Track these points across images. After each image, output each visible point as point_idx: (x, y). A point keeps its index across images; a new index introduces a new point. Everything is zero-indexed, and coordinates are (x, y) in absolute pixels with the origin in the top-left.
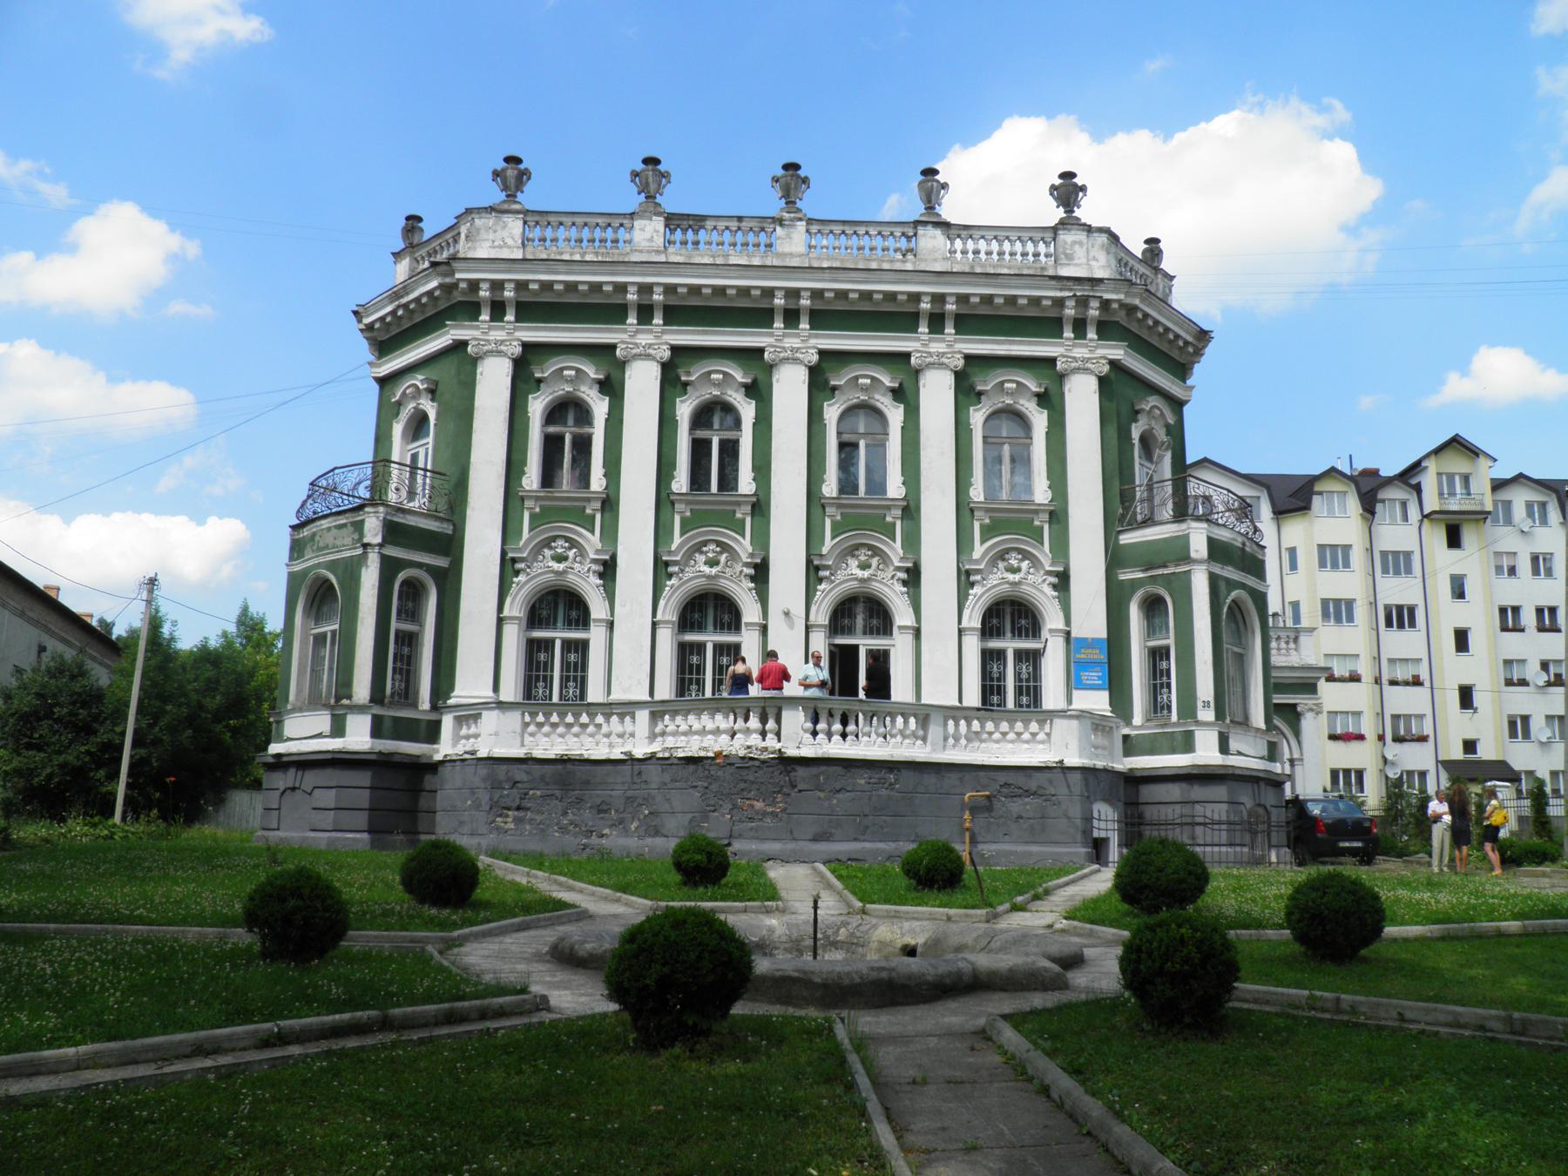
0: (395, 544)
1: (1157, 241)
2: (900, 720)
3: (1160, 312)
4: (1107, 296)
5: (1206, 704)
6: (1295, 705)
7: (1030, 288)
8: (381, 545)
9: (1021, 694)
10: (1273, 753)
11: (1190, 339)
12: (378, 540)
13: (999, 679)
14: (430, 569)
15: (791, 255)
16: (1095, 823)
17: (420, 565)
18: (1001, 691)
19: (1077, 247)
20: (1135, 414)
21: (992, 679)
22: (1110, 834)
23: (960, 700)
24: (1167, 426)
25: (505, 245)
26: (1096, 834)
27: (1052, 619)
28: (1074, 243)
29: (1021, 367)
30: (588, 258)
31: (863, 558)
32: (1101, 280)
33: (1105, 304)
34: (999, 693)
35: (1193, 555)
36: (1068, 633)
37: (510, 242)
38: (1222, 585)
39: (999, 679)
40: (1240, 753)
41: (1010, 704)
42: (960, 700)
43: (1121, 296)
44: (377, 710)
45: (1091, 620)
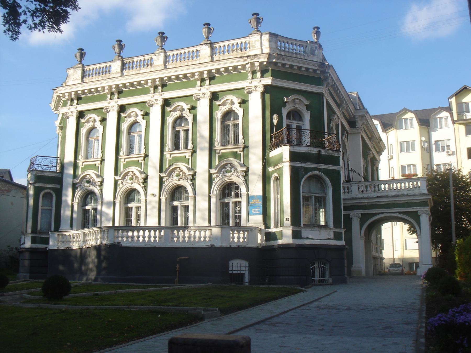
0: (40, 182)
1: (318, 28)
2: (152, 232)
3: (291, 61)
4: (261, 60)
5: (287, 220)
6: (417, 211)
7: (232, 62)
8: (34, 183)
9: (236, 218)
10: (337, 236)
11: (316, 68)
12: (33, 182)
13: (238, 213)
14: (53, 189)
15: (158, 66)
16: (231, 269)
17: (49, 188)
18: (228, 217)
19: (256, 42)
20: (284, 104)
21: (226, 214)
22: (244, 272)
23: (210, 222)
24: (307, 105)
25: (77, 79)
26: (231, 272)
27: (243, 189)
28: (256, 41)
29: (233, 94)
30: (100, 79)
31: (177, 173)
32: (257, 55)
33: (261, 63)
34: (239, 219)
35: (284, 160)
36: (248, 194)
37: (78, 78)
38: (302, 171)
39: (238, 213)
40: (308, 238)
41: (231, 224)
42: (210, 222)
43: (266, 60)
44: (33, 235)
45: (256, 188)
